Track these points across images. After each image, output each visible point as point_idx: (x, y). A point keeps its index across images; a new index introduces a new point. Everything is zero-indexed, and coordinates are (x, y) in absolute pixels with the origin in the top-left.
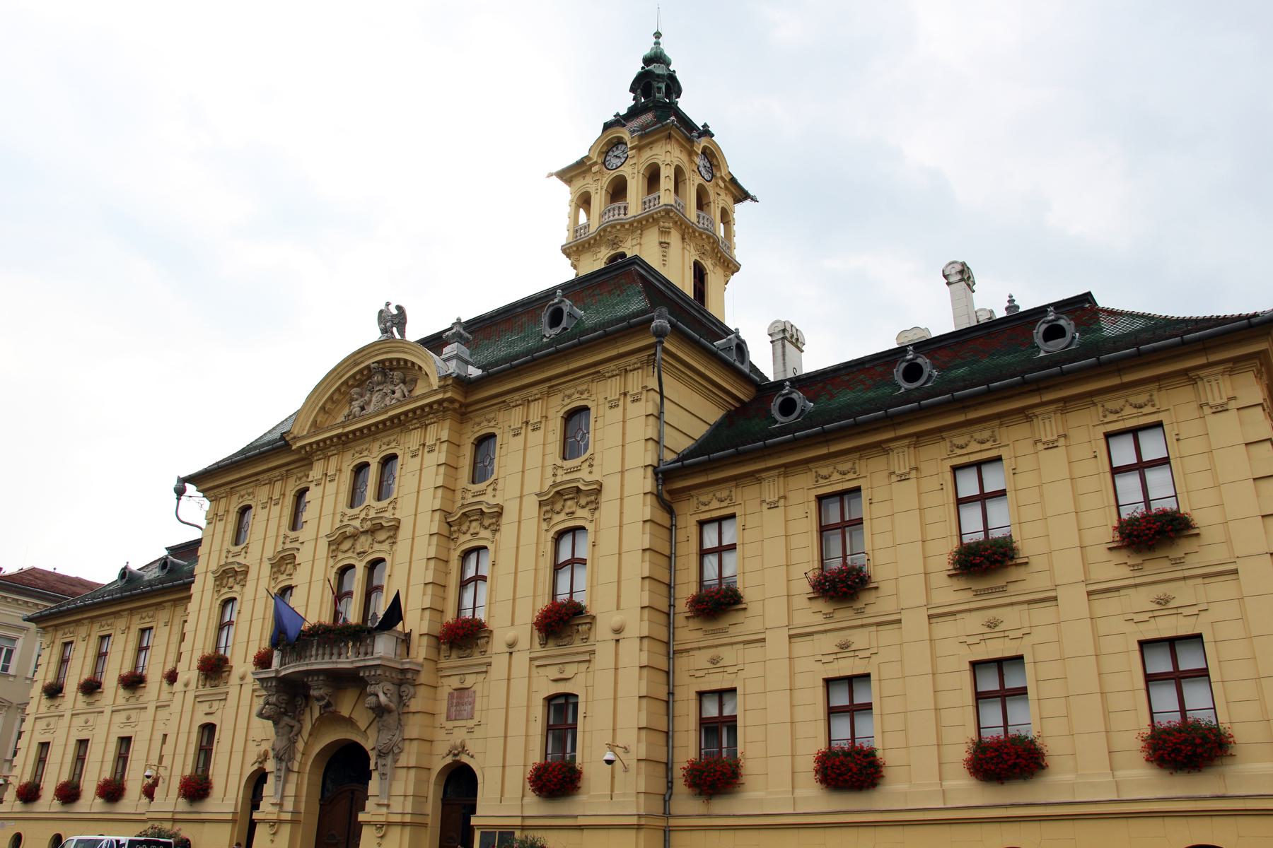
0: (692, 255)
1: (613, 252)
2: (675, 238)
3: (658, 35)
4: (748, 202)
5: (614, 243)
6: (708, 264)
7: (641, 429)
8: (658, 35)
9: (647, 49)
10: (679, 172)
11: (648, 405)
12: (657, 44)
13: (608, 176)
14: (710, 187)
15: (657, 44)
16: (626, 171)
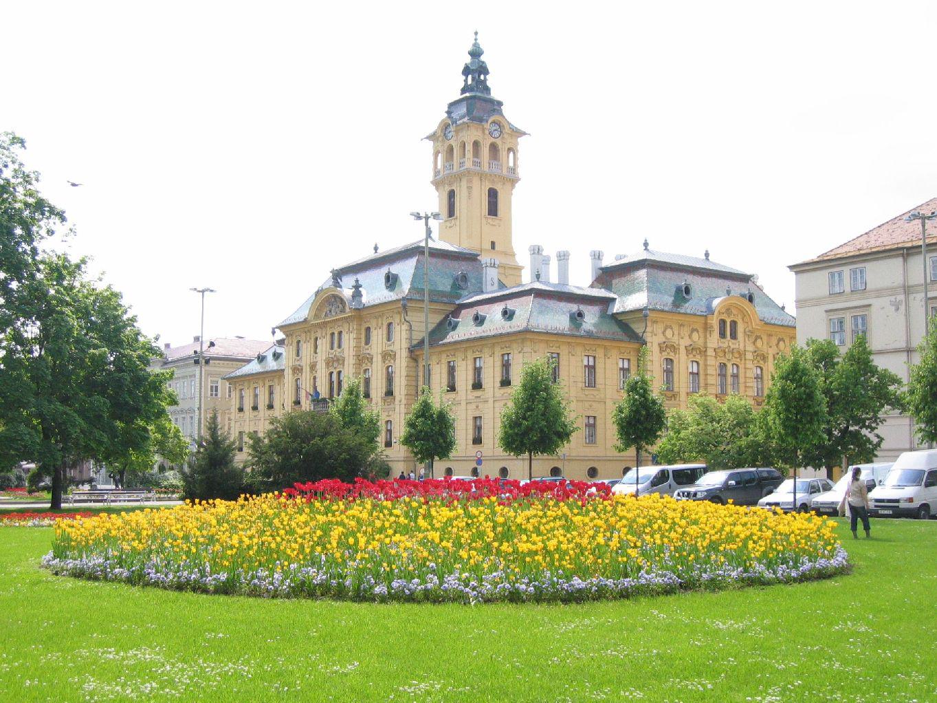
0: (488, 185)
1: (450, 189)
2: (476, 182)
3: (476, 33)
4: (524, 137)
5: (450, 185)
6: (498, 187)
7: (405, 335)
8: (476, 33)
9: (470, 48)
10: (476, 144)
11: (405, 327)
12: (476, 40)
13: (447, 143)
14: (498, 142)
15: (476, 40)
16: (452, 142)
